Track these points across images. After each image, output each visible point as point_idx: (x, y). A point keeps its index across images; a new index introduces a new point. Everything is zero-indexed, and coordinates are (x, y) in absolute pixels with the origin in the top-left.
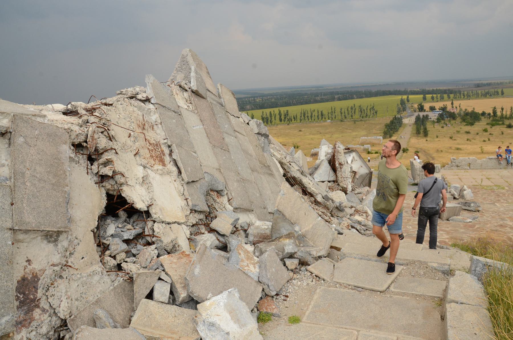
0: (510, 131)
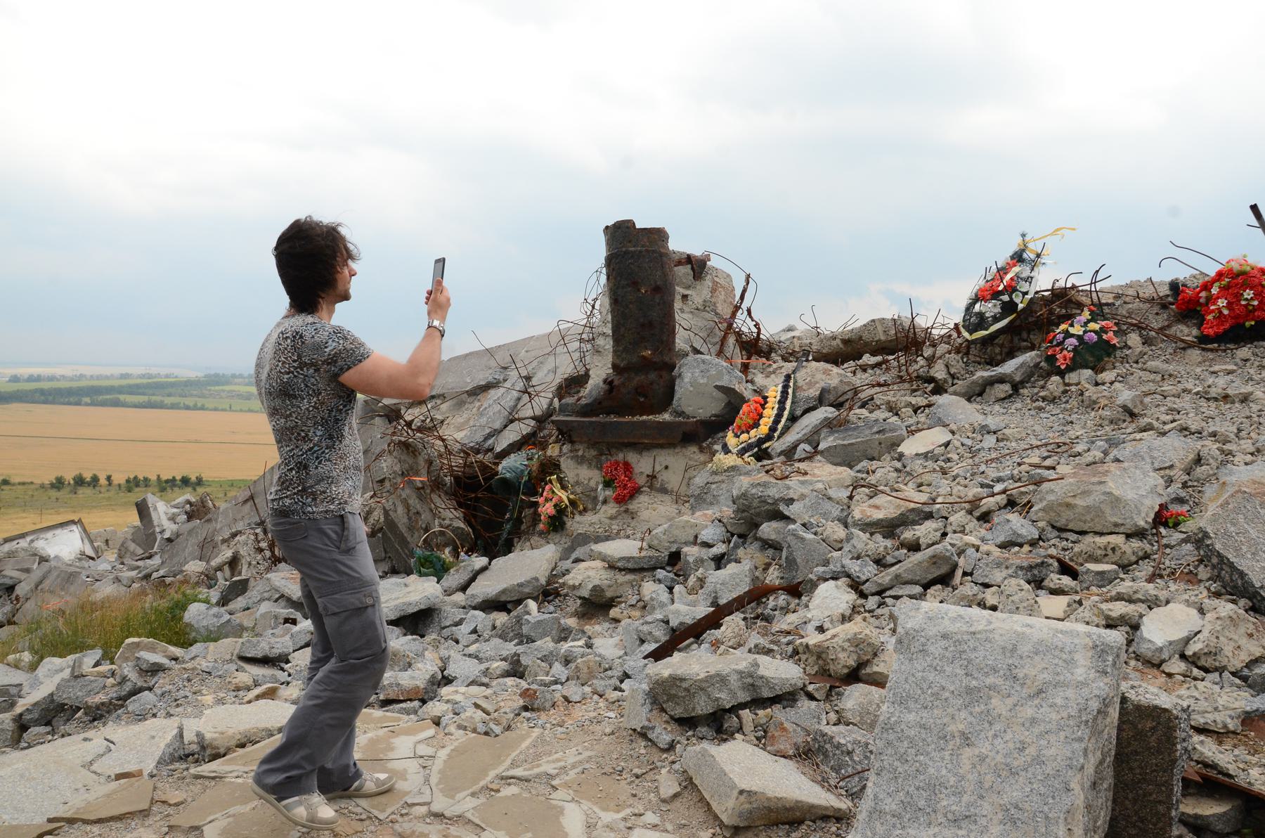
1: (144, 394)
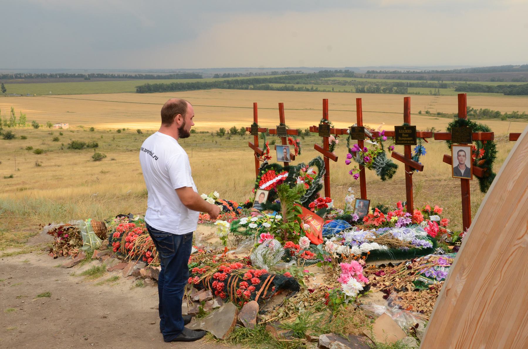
1: (284, 83)
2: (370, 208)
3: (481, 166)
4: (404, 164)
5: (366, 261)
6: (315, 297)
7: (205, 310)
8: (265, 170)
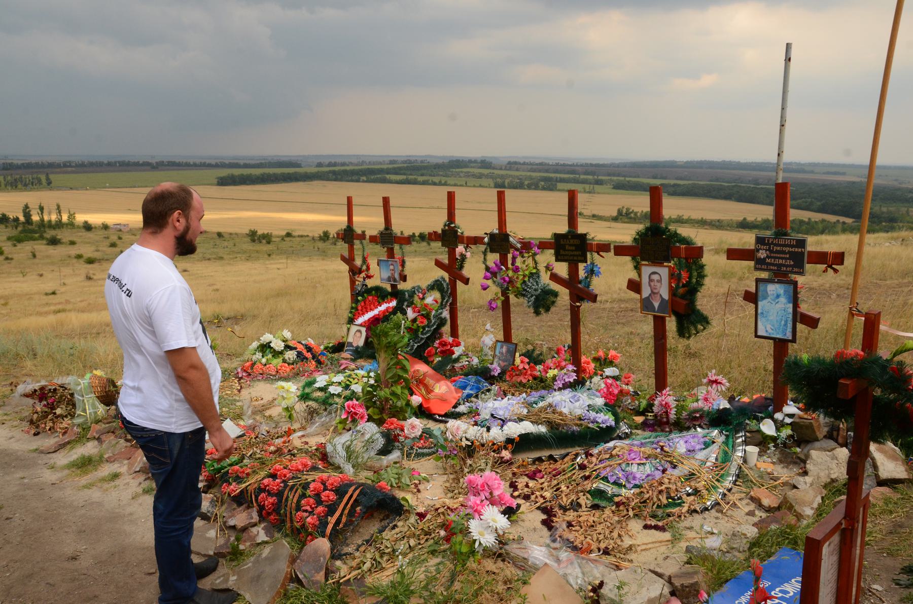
0: (53, 251)
1: (404, 174)
2: (517, 354)
3: (683, 297)
4: (567, 291)
5: (513, 452)
6: (427, 530)
7: (241, 547)
8: (363, 296)
